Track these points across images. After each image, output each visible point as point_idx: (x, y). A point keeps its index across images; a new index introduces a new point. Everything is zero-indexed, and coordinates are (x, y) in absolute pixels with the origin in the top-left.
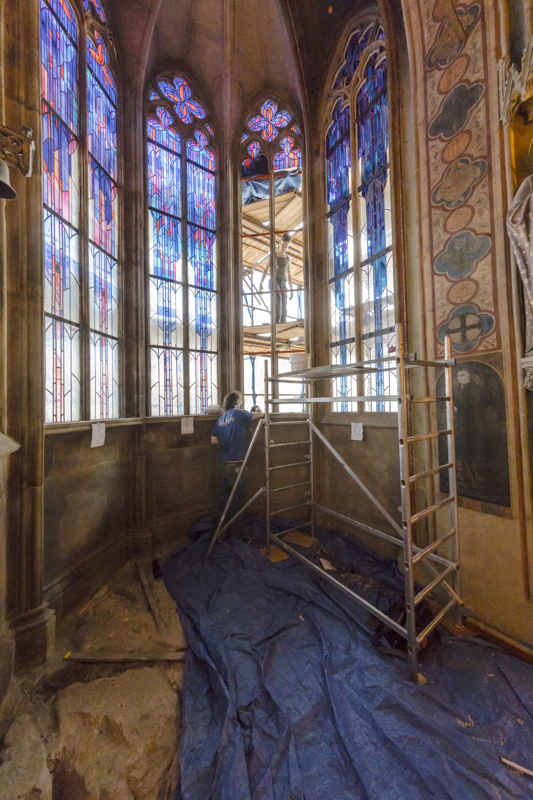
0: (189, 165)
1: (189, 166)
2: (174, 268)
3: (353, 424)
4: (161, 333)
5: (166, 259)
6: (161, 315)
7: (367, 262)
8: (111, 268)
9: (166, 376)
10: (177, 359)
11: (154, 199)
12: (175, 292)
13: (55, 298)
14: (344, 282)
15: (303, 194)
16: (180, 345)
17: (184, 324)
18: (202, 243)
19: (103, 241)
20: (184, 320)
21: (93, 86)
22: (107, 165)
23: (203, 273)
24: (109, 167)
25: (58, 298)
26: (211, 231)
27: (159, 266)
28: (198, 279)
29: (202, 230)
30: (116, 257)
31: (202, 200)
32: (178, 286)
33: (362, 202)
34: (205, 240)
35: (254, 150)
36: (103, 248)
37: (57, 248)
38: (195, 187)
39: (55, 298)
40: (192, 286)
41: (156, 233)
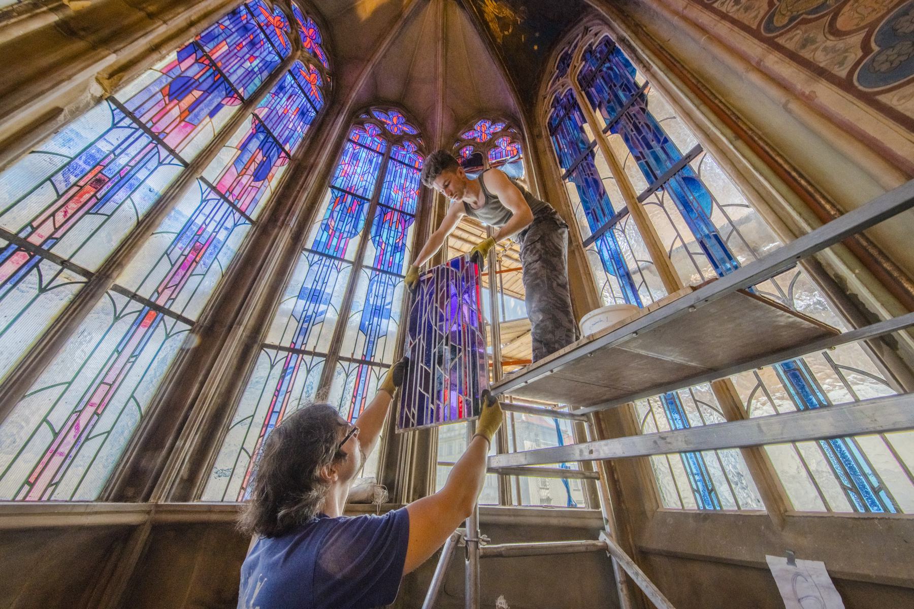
0: (390, 163)
1: (390, 163)
2: (346, 244)
3: (776, 564)
4: (294, 324)
5: (337, 234)
6: (302, 298)
7: (649, 192)
8: (235, 225)
9: (273, 404)
10: (309, 371)
11: (339, 180)
12: (339, 272)
13: (53, 215)
14: (613, 236)
15: (527, 180)
16: (324, 348)
17: (340, 315)
18: (394, 225)
19: (237, 192)
20: (341, 310)
21: (292, 86)
22: (284, 137)
23: (388, 254)
24: (287, 140)
25: (60, 217)
26: (407, 214)
27: (324, 240)
28: (379, 260)
29: (396, 213)
30: (254, 217)
31: (403, 188)
32: (345, 265)
33: (616, 141)
34: (399, 221)
35: (467, 152)
36: (230, 198)
37: (123, 160)
38: (395, 176)
39: (53, 215)
40: (367, 267)
41: (331, 207)
